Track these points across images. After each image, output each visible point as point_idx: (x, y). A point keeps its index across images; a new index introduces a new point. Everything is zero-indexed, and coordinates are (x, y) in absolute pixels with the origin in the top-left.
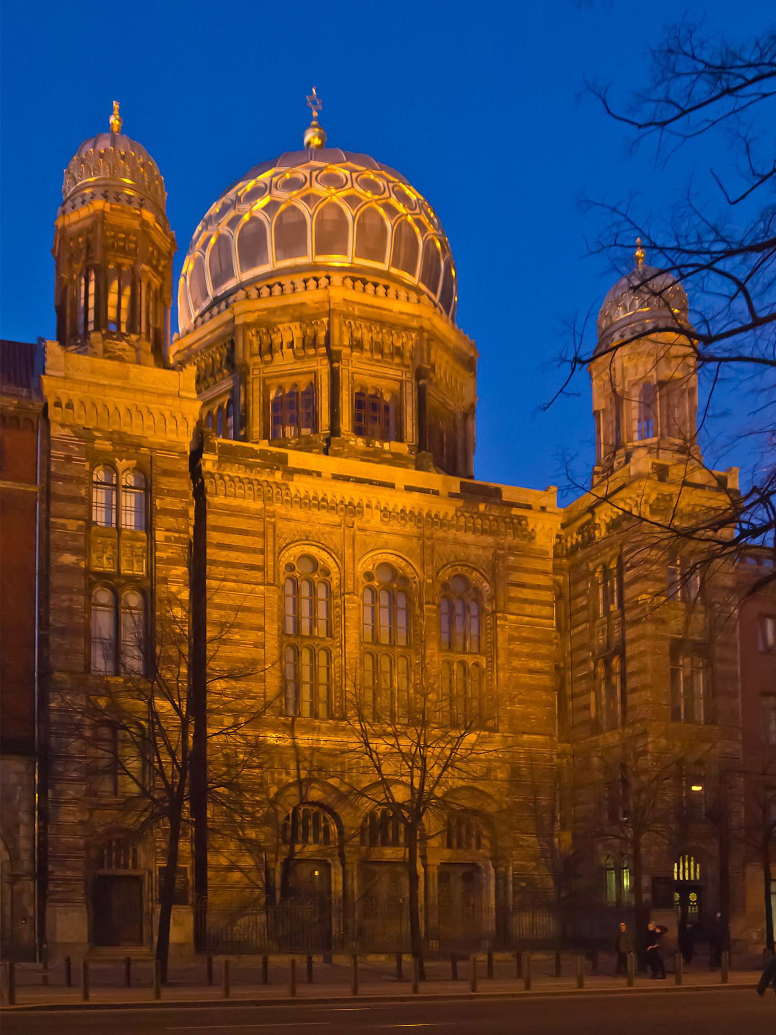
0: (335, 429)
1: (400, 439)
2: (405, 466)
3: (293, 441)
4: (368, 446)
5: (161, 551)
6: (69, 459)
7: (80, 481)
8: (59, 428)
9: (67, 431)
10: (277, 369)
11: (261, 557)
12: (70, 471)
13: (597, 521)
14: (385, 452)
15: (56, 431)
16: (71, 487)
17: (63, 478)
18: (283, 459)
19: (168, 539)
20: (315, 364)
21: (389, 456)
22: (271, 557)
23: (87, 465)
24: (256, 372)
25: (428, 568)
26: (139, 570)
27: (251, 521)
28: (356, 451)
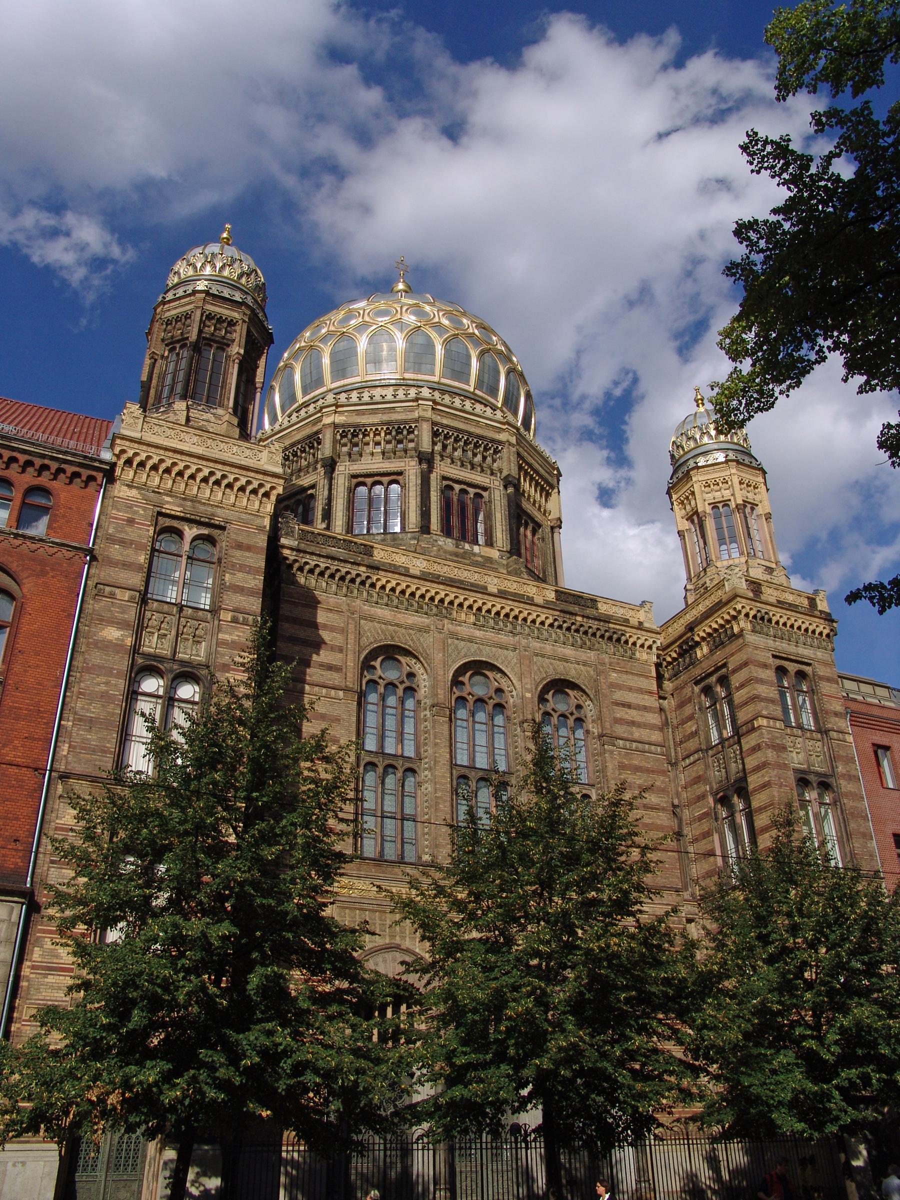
0: (425, 528)
1: (490, 543)
2: (495, 570)
3: (379, 538)
4: (457, 547)
5: (225, 633)
6: (131, 521)
7: (139, 547)
8: (125, 488)
9: (134, 493)
10: (365, 467)
11: (340, 655)
12: (132, 533)
13: (697, 639)
14: (475, 555)
15: (120, 491)
16: (130, 551)
17: (122, 542)
18: (368, 550)
19: (235, 620)
20: (403, 464)
21: (480, 559)
22: (350, 656)
23: (152, 529)
24: (342, 468)
25: (526, 680)
26: (198, 653)
27: (330, 615)
28: (446, 552)
